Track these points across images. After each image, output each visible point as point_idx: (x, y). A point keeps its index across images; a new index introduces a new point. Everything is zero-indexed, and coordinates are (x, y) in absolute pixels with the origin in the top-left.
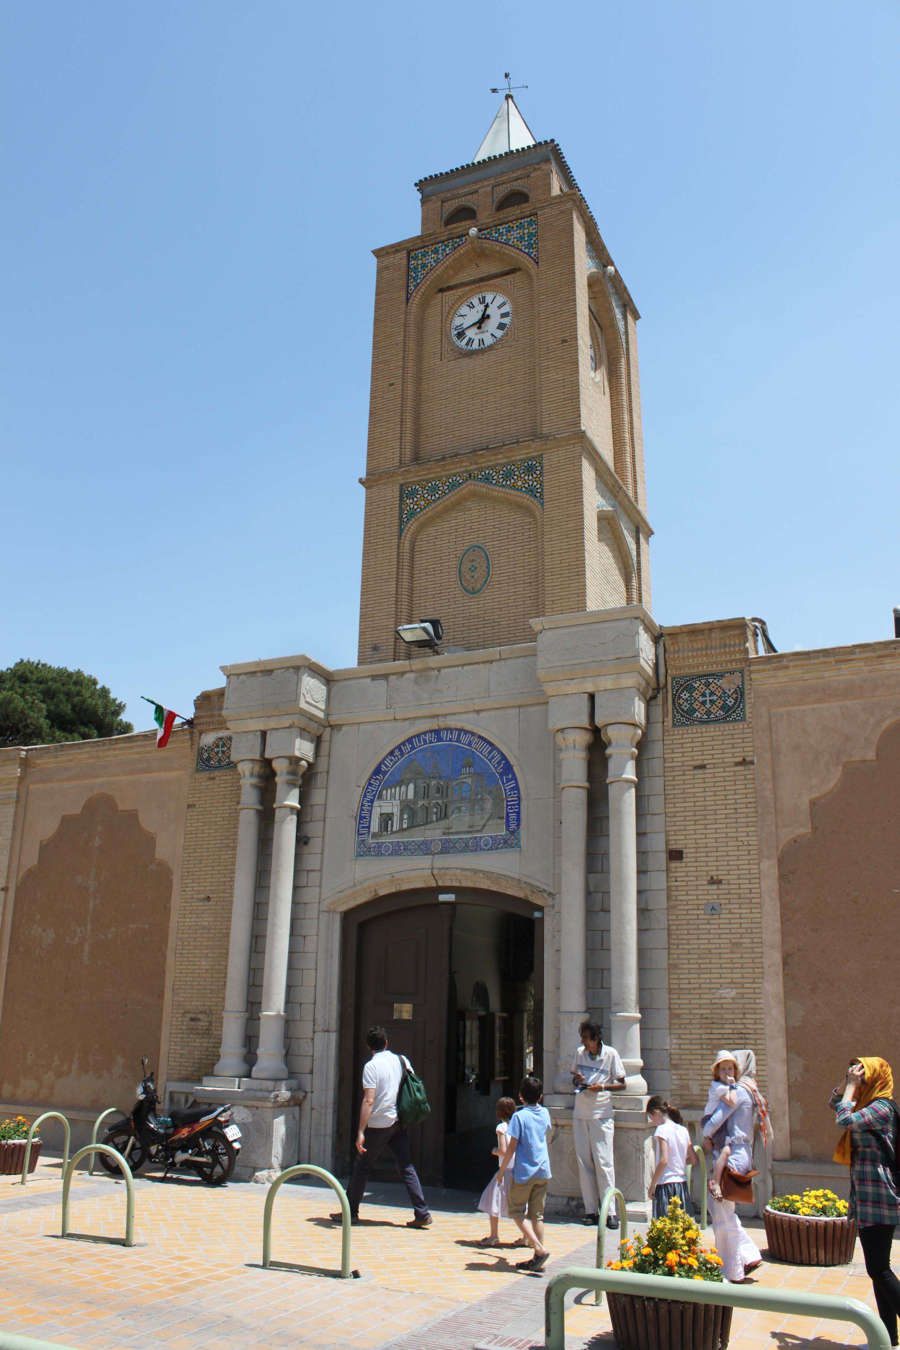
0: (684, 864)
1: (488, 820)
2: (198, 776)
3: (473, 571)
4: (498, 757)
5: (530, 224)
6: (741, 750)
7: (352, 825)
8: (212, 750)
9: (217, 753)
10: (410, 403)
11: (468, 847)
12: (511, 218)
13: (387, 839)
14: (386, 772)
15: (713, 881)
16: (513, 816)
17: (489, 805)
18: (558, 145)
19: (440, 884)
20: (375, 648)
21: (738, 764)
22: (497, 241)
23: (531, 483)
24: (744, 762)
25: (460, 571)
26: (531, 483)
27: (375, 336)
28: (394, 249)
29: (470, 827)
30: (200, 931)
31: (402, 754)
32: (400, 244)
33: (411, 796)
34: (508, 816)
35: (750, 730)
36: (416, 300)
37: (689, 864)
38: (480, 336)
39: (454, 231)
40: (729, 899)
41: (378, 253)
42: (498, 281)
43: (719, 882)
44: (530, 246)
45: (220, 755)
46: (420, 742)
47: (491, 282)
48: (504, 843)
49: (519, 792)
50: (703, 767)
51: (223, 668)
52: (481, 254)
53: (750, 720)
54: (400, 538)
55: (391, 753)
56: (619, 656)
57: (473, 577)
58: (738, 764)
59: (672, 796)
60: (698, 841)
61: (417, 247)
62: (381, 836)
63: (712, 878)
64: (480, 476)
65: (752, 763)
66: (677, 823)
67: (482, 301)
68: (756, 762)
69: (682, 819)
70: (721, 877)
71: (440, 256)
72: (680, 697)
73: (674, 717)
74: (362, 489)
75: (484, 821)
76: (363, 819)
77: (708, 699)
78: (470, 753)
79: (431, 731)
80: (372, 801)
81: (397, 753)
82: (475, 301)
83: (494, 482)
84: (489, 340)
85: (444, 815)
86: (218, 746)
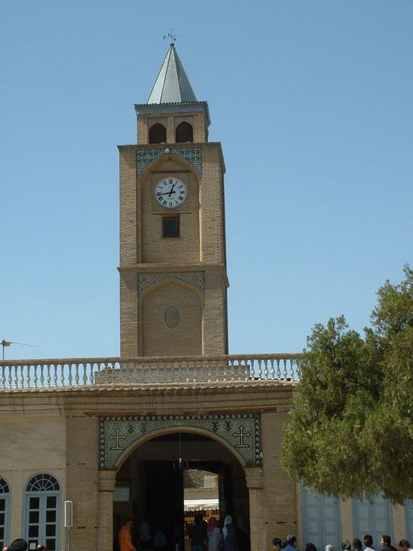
38: (170, 201)
41: (120, 148)
67: (171, 182)
82: (168, 182)
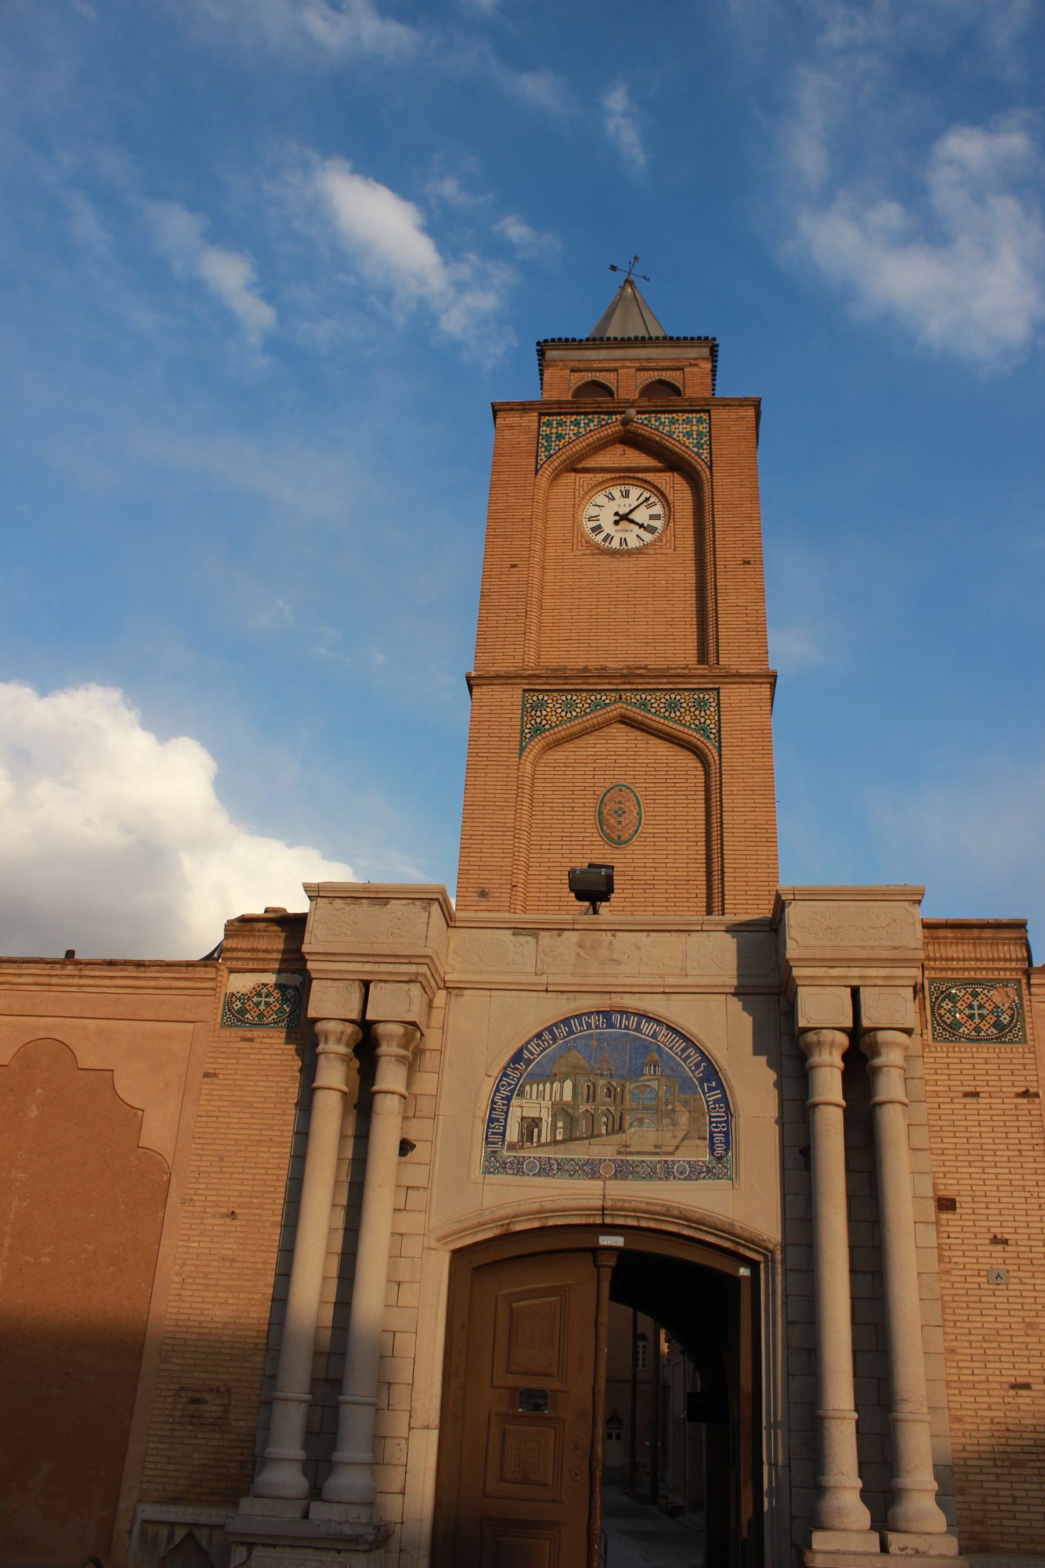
0: (957, 1216)
1: (683, 1139)
2: (226, 1033)
3: (620, 816)
4: (696, 1057)
5: (700, 421)
6: (1023, 1078)
7: (480, 1129)
8: (249, 999)
9: (258, 1004)
11: (655, 1173)
13: (530, 1153)
14: (529, 1062)
15: (995, 1240)
16: (719, 1137)
17: (684, 1119)
18: (717, 346)
19: (608, 1221)
20: (483, 894)
21: (1019, 1095)
22: (657, 430)
23: (702, 720)
24: (1026, 1094)
25: (600, 813)
26: (702, 720)
29: (656, 1146)
30: (215, 1264)
31: (555, 1039)
32: (530, 403)
33: (568, 1096)
34: (712, 1137)
35: (1031, 1056)
36: (547, 472)
37: (964, 1217)
38: (623, 535)
40: (1019, 1265)
42: (649, 477)
43: (1005, 1242)
44: (700, 446)
45: (262, 1008)
46: (581, 1025)
47: (640, 475)
48: (708, 1172)
49: (728, 1106)
50: (976, 1095)
51: (307, 888)
52: (631, 439)
53: (1032, 1043)
54: (520, 758)
55: (539, 1036)
56: (897, 944)
57: (620, 823)
58: (1019, 1095)
59: (938, 1129)
60: (974, 1188)
62: (522, 1148)
63: (995, 1237)
64: (634, 700)
65: (1037, 1095)
66: (946, 1163)
68: (1041, 1095)
69: (953, 1158)
70: (1007, 1236)
72: (940, 1007)
73: (934, 1030)
75: (678, 1140)
76: (495, 1122)
77: (976, 1012)
78: (655, 1047)
79: (598, 1013)
80: (509, 1099)
81: (546, 1036)
83: (653, 710)
84: (633, 543)
85: (618, 1127)
86: (259, 995)
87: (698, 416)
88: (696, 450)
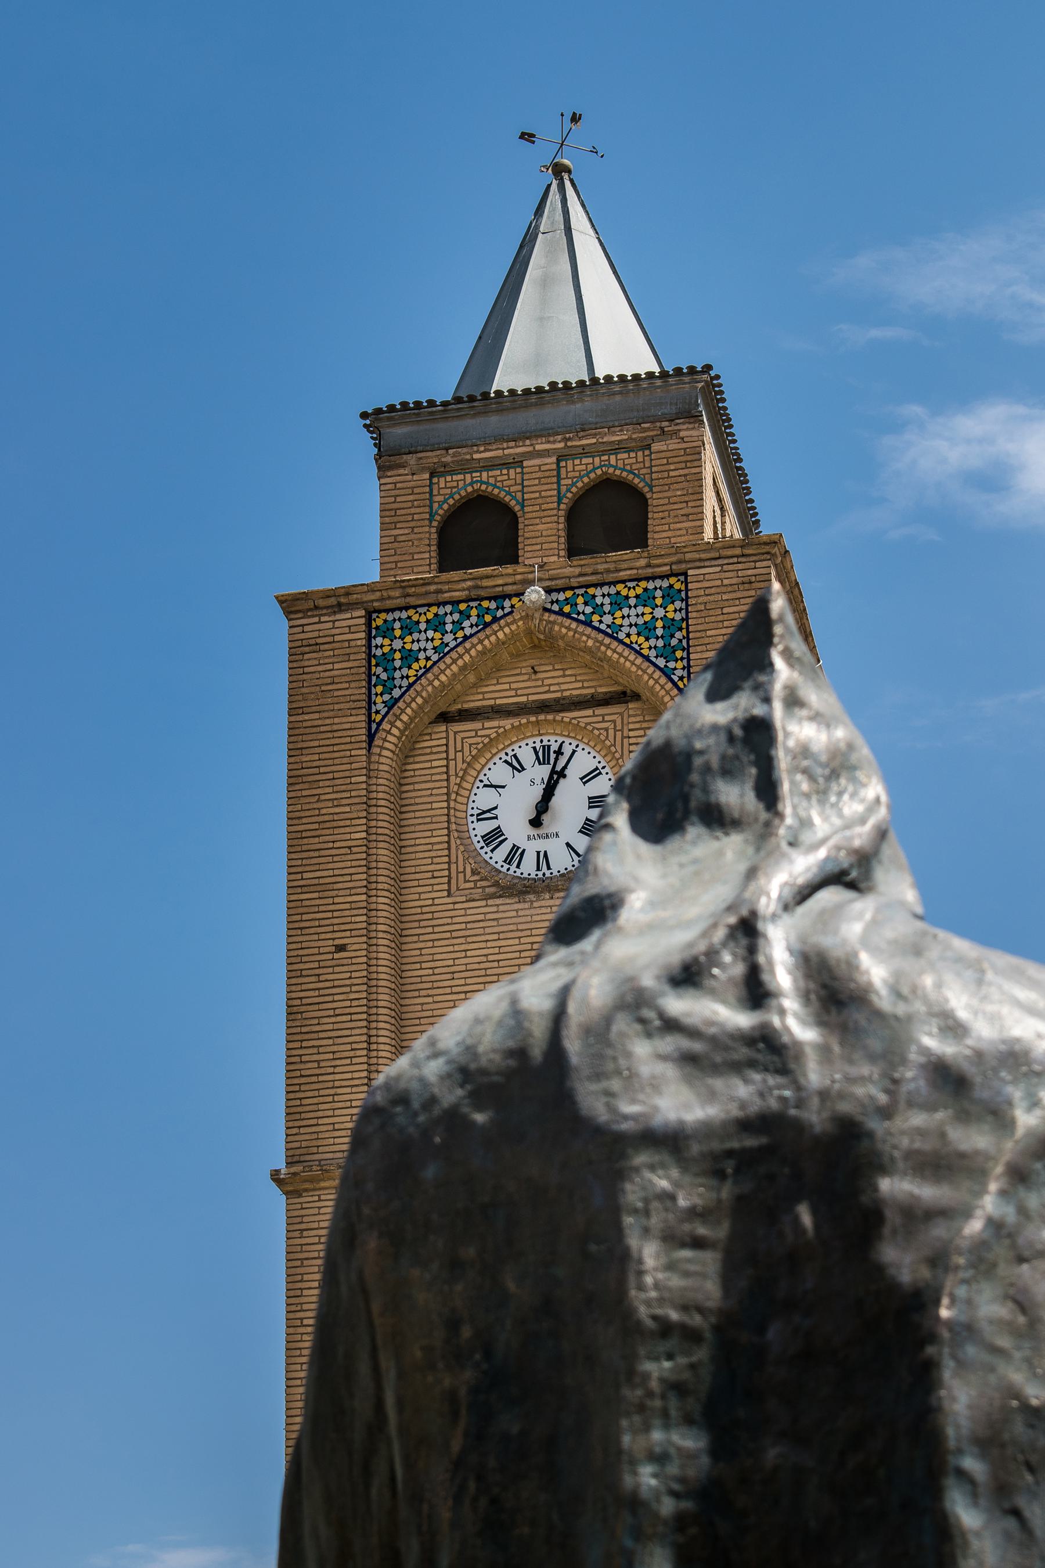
5: (669, 595)
10: (384, 998)
12: (623, 575)
18: (718, 377)
22: (588, 624)
27: (292, 819)
28: (332, 601)
32: (348, 591)
36: (390, 738)
38: (541, 845)
39: (485, 583)
44: (667, 652)
47: (567, 716)
52: (542, 646)
61: (389, 604)
71: (448, 638)
74: (278, 1200)
82: (526, 755)
87: (665, 584)
88: (661, 662)
